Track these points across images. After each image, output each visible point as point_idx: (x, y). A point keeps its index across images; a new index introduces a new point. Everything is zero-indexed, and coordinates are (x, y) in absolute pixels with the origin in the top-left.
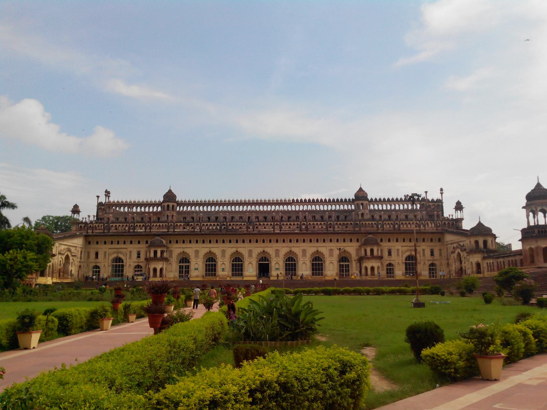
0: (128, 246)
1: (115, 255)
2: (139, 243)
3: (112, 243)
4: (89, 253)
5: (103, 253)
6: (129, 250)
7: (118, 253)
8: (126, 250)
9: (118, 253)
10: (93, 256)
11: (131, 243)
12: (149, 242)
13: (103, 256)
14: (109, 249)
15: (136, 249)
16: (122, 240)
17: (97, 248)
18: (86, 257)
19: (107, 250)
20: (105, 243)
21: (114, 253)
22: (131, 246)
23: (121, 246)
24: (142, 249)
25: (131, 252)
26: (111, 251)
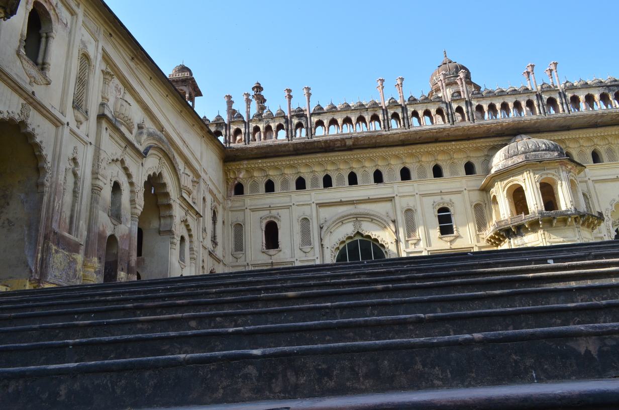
0: (393, 187)
1: (348, 230)
2: (437, 172)
3: (327, 182)
4: (239, 228)
5: (297, 228)
6: (402, 203)
7: (358, 218)
8: (387, 206)
9: (358, 218)
10: (255, 237)
11: (405, 175)
12: (478, 168)
13: (298, 238)
14: (321, 205)
15: (428, 201)
16: (365, 167)
17: (270, 208)
18: (231, 245)
19: (311, 212)
20: (301, 184)
21: (342, 220)
22: (406, 187)
23: (366, 189)
24: (455, 198)
25: (409, 212)
26: (327, 213)
